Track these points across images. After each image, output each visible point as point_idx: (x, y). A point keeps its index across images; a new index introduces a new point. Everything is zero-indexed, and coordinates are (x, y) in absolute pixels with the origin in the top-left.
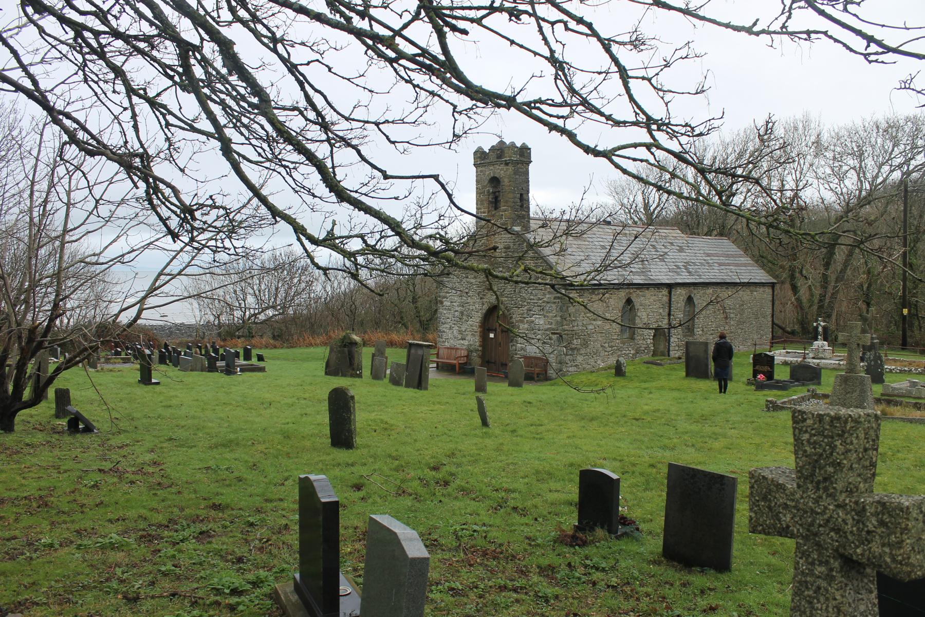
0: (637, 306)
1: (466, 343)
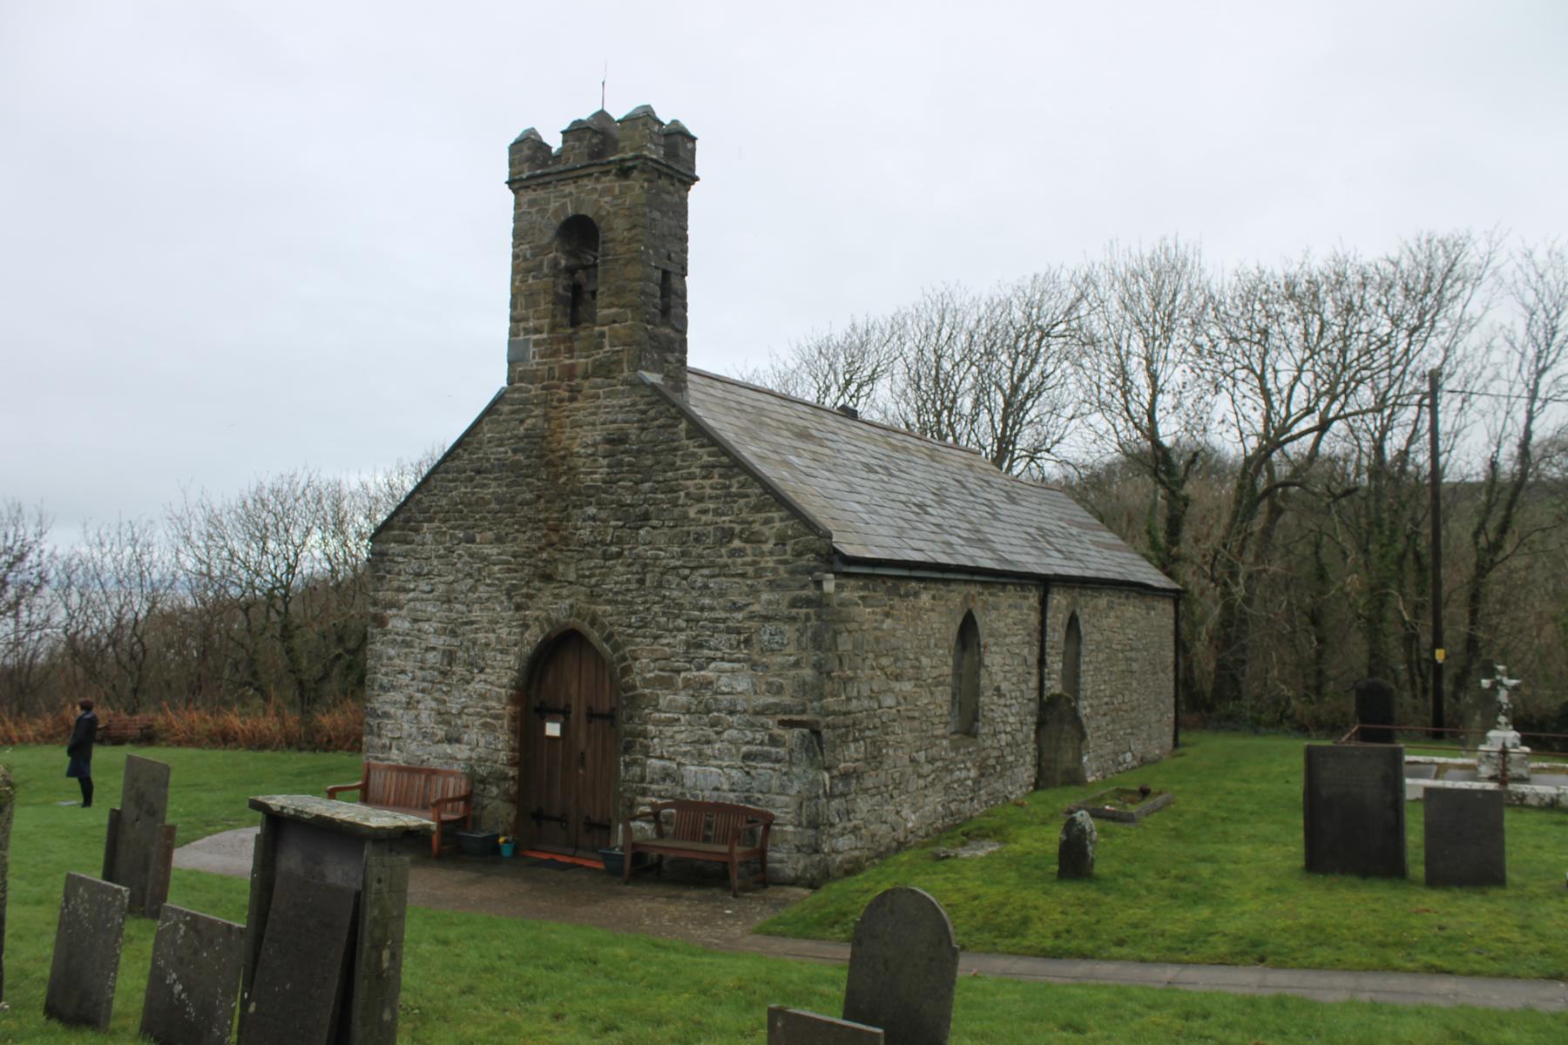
0: (983, 630)
1: (462, 751)
